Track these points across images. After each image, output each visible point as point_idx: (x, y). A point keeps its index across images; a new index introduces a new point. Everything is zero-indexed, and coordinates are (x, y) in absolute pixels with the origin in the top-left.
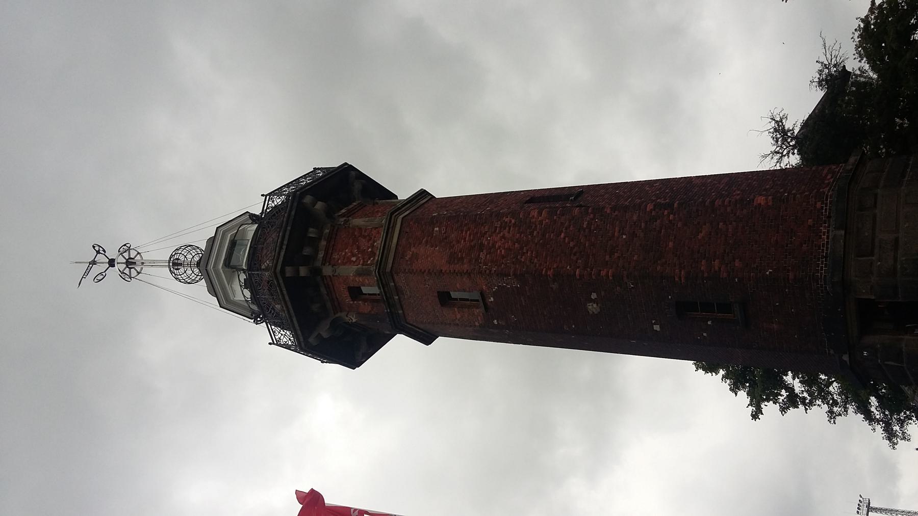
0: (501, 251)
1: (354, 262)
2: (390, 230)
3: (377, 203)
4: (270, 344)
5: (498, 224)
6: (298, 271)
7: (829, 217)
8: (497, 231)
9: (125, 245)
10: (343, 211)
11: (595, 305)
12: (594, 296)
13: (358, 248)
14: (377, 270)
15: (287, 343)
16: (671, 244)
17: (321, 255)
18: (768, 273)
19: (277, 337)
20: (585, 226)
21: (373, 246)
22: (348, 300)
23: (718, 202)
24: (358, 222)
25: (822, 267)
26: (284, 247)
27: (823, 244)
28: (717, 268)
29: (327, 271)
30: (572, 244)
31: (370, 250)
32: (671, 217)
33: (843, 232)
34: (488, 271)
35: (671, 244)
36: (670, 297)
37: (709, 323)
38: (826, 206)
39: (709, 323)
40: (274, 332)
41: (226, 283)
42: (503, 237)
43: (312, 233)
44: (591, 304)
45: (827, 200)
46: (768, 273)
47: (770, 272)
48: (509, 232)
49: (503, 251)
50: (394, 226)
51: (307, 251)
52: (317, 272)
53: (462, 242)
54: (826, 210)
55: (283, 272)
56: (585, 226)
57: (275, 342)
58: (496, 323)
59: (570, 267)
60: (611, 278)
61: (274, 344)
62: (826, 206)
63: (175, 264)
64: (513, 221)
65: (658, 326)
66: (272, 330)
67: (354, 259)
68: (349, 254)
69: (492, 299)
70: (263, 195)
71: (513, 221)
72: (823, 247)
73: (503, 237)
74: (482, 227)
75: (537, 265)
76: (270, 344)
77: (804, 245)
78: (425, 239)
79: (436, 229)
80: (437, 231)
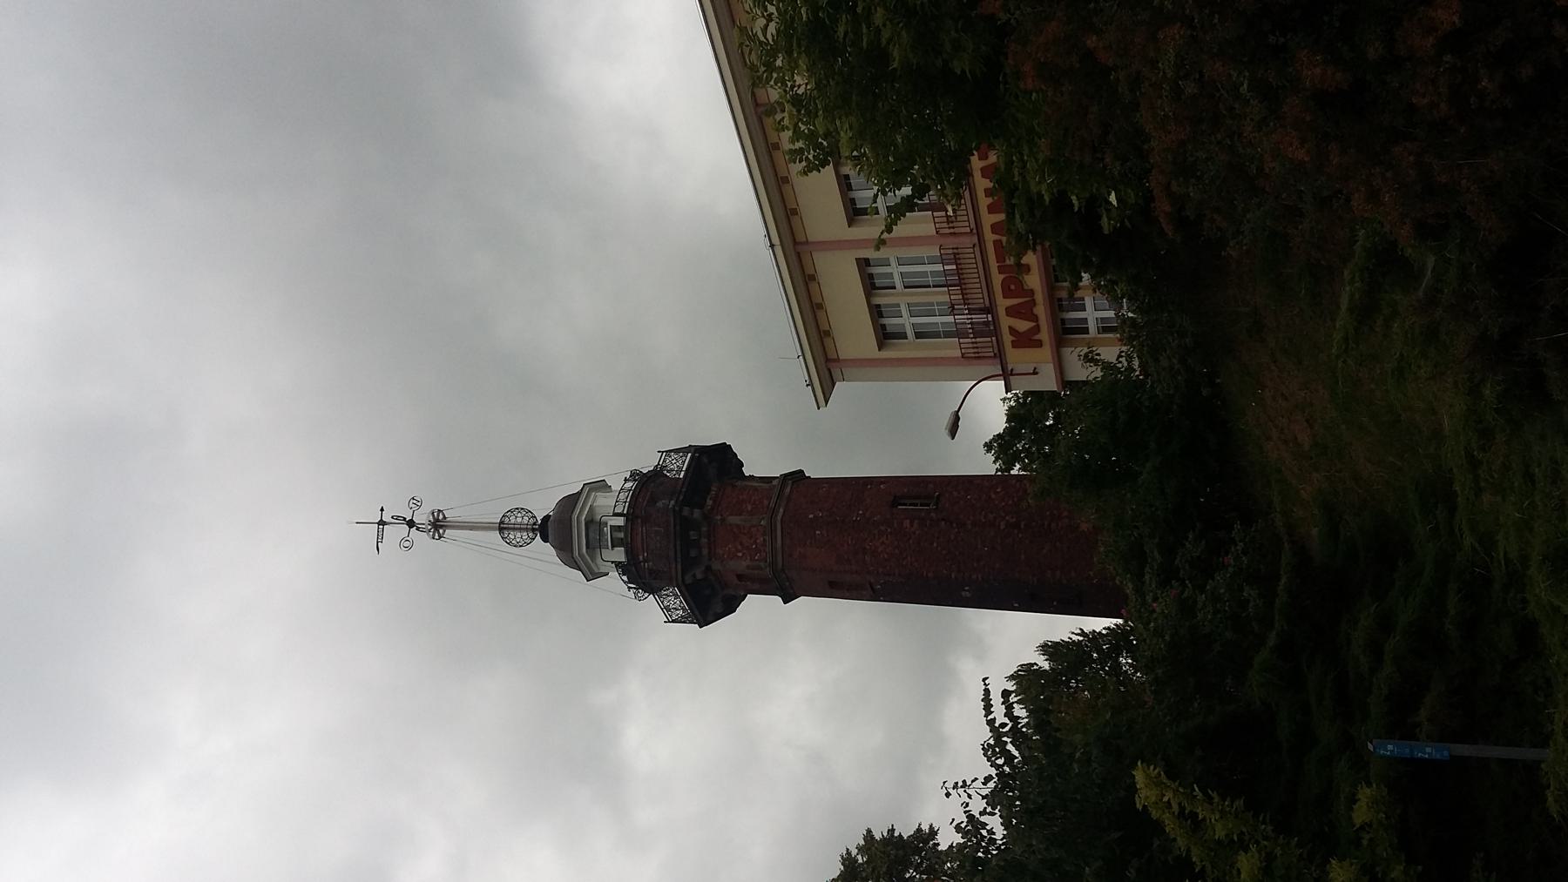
3: (736, 486)
5: (876, 532)
6: (694, 576)
9: (413, 498)
10: (709, 502)
13: (741, 544)
16: (1023, 557)
17: (705, 552)
21: (755, 542)
22: (736, 581)
23: (1053, 525)
24: (734, 520)
26: (679, 560)
29: (716, 566)
30: (944, 552)
31: (754, 546)
32: (1020, 536)
35: (1023, 557)
39: (1055, 603)
41: (590, 562)
42: (883, 543)
43: (693, 535)
48: (887, 539)
50: (776, 530)
51: (693, 553)
52: (708, 568)
55: (683, 580)
61: (669, 622)
63: (502, 528)
64: (889, 530)
67: (740, 554)
71: (889, 530)
73: (883, 543)
79: (818, 532)
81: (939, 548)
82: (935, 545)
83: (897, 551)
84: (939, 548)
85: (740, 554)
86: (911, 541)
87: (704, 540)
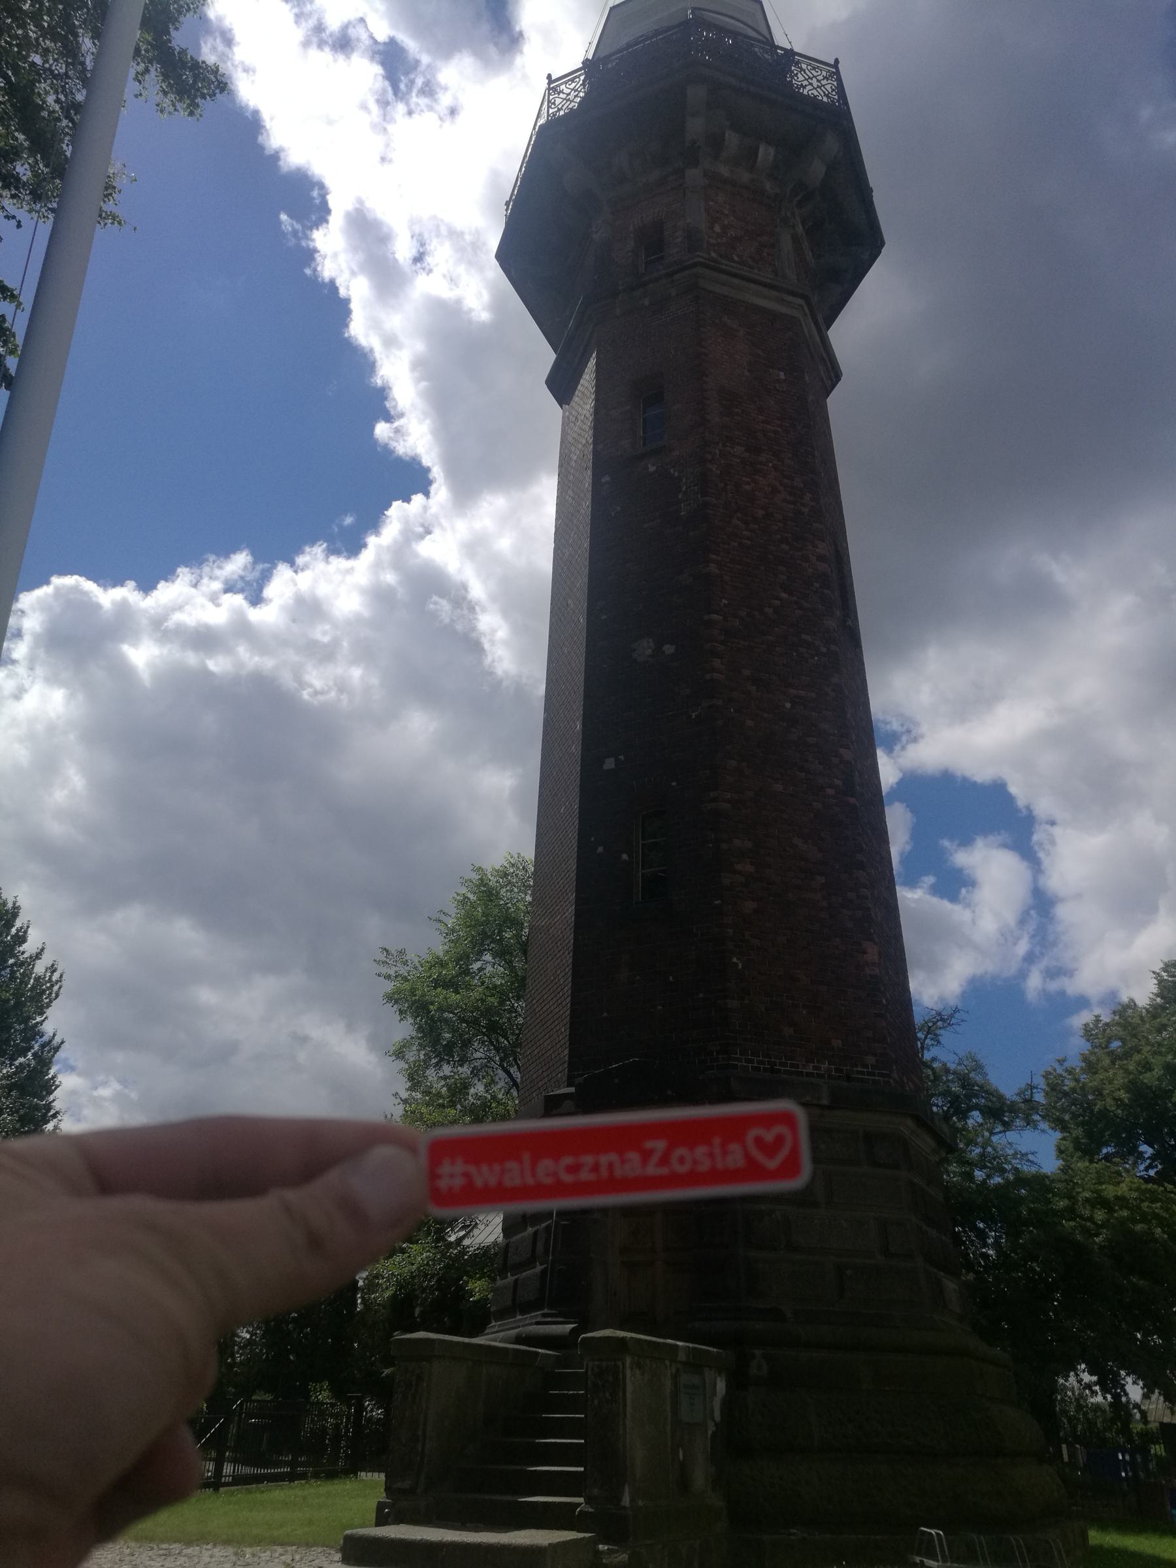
0: (748, 484)
1: (712, 228)
2: (774, 293)
4: (549, 76)
7: (849, 1078)
8: (786, 481)
11: (649, 652)
12: (669, 649)
14: (702, 260)
15: (553, 106)
17: (724, 171)
18: (735, 960)
19: (563, 87)
20: (803, 636)
25: (751, 1061)
27: (797, 1066)
28: (739, 867)
32: (830, 791)
33: (825, 1102)
34: (709, 457)
35: (779, 787)
36: (674, 784)
37: (625, 857)
38: (869, 1074)
39: (625, 857)
40: (572, 80)
44: (651, 644)
45: (880, 1075)
46: (735, 960)
47: (737, 964)
49: (747, 487)
53: (760, 417)
54: (862, 1073)
56: (803, 636)
57: (552, 86)
58: (603, 480)
59: (724, 604)
60: (708, 676)
61: (549, 84)
62: (869, 1074)
65: (613, 766)
66: (576, 77)
67: (717, 229)
68: (726, 222)
69: (652, 469)
70: (837, 61)
71: (805, 510)
72: (792, 1066)
74: (790, 456)
75: (726, 547)
76: (549, 76)
77: (792, 1029)
78: (760, 352)
80: (778, 375)
81: (777, 603)
82: (784, 595)
83: (761, 513)
84: (777, 603)
85: (717, 229)
86: (785, 547)
87: (746, 177)
